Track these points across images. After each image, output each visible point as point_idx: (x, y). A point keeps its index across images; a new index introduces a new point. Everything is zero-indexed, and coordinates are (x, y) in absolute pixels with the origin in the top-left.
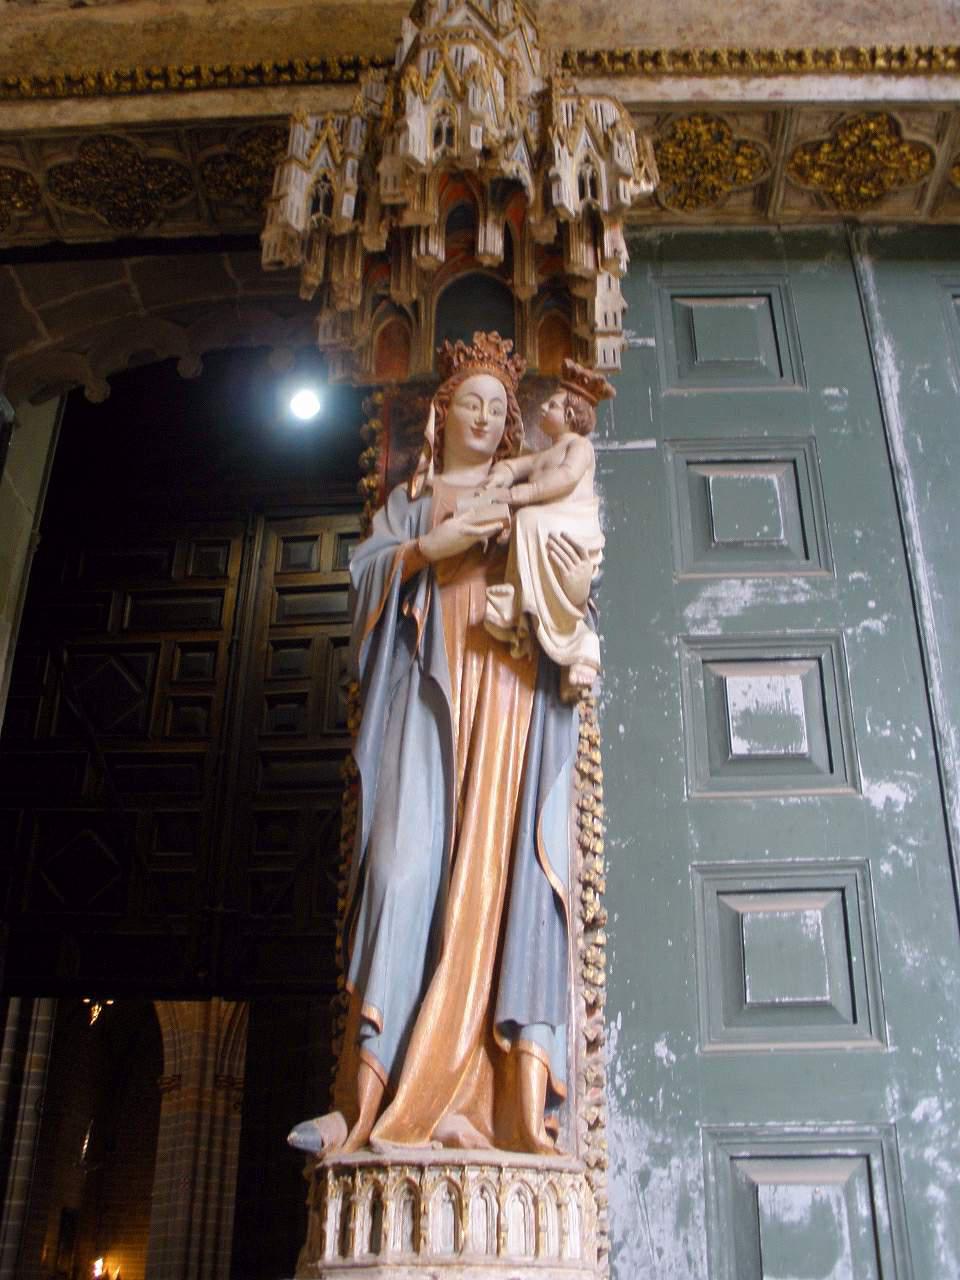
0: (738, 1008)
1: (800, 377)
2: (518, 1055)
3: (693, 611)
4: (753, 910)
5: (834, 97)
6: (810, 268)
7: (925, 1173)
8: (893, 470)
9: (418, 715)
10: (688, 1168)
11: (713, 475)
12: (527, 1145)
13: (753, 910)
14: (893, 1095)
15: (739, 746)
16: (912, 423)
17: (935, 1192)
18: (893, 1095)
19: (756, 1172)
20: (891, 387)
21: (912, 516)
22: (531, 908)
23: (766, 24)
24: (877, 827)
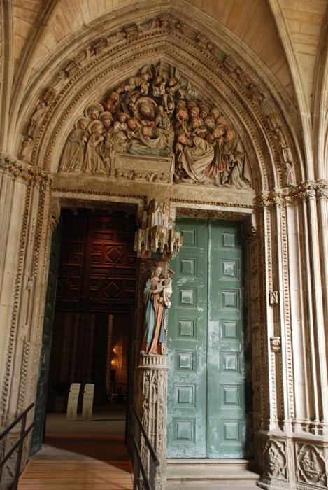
0: (179, 335)
1: (197, 246)
2: (161, 346)
3: (178, 282)
4: (182, 323)
5: (208, 209)
6: (202, 226)
7: (200, 355)
8: (208, 263)
9: (152, 310)
10: (172, 354)
11: (183, 261)
12: (161, 354)
13: (182, 323)
14: (197, 347)
15: (183, 302)
16: (212, 255)
17: (200, 358)
18: (197, 347)
19: (180, 354)
20: (210, 249)
21: (209, 271)
22: (162, 331)
24: (198, 314)
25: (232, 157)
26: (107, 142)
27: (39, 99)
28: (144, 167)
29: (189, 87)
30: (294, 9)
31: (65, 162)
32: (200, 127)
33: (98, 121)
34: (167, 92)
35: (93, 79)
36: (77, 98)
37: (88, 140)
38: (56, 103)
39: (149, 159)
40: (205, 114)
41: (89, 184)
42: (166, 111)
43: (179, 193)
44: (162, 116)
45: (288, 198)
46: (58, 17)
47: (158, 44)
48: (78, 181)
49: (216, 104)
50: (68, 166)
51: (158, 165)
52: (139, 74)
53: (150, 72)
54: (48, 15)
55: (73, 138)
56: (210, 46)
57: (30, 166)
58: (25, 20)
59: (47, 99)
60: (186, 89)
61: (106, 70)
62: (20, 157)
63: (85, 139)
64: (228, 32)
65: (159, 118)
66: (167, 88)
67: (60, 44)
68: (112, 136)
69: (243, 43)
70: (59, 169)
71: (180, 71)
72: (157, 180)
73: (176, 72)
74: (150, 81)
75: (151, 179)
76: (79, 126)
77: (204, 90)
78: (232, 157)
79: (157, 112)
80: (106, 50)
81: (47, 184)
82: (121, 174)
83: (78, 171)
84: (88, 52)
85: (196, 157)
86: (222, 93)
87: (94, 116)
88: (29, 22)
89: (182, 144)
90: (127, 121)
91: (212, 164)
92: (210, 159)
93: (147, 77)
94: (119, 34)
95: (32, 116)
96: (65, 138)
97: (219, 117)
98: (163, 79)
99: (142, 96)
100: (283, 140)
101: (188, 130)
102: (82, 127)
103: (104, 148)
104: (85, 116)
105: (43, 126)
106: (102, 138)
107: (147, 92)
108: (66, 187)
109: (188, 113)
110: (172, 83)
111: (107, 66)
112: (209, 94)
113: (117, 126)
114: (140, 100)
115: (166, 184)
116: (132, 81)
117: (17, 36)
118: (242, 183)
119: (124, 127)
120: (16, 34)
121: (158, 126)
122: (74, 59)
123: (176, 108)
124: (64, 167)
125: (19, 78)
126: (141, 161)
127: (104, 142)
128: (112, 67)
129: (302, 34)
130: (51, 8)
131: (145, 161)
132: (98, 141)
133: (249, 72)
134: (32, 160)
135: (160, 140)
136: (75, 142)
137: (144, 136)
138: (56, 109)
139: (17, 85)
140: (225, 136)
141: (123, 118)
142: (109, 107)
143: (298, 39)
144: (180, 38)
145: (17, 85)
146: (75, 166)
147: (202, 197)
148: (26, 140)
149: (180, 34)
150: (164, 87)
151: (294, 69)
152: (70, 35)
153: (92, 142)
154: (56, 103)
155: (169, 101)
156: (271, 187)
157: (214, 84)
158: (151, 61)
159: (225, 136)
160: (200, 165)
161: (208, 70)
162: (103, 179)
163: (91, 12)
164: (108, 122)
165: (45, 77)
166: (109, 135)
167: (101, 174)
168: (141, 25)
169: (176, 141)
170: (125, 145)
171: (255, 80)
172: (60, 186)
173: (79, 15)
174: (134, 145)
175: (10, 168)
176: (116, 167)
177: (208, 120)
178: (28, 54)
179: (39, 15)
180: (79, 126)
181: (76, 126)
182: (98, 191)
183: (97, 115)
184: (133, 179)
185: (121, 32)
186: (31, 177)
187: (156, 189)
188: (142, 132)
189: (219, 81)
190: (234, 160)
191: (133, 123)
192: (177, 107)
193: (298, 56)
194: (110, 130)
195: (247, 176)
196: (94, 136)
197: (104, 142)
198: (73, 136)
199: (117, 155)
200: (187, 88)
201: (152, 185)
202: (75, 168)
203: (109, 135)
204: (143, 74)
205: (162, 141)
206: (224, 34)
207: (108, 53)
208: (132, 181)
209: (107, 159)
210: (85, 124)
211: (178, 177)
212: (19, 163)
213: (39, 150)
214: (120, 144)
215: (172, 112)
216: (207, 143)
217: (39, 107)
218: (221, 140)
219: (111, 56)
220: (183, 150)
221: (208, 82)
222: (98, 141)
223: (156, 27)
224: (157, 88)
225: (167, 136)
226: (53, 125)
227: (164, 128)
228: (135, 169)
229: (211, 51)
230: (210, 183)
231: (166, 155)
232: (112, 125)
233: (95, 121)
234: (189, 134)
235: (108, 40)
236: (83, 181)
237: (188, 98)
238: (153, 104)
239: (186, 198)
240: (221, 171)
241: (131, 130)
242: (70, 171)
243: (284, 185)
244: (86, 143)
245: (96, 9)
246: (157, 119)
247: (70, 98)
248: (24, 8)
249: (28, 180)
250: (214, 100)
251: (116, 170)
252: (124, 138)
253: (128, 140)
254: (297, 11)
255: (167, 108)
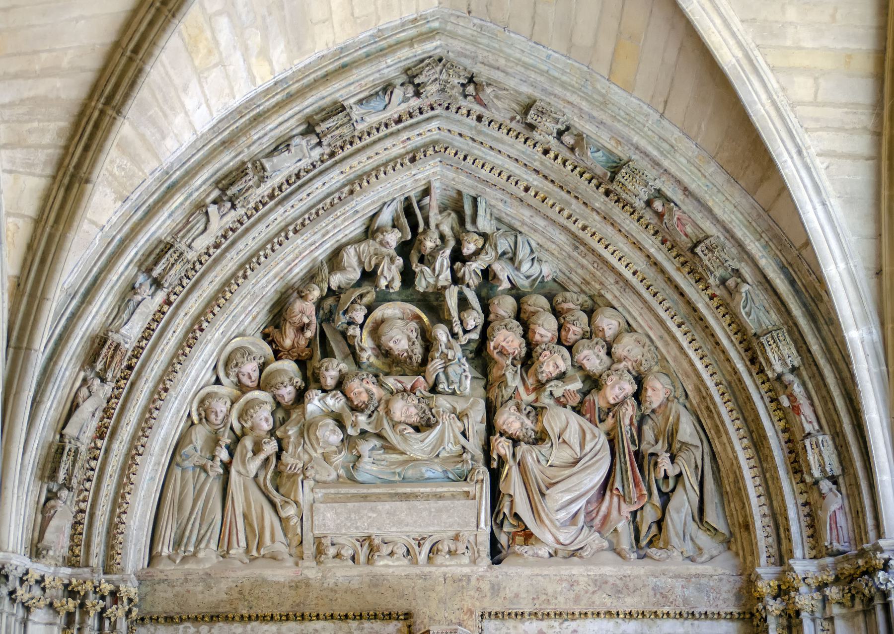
23: (571, 595)
25: (664, 462)
26: (287, 458)
27: (82, 368)
28: (400, 522)
29: (523, 252)
30: (789, 43)
31: (168, 533)
32: (562, 376)
33: (257, 394)
34: (456, 280)
35: (234, 275)
36: (189, 340)
37: (231, 455)
38: (130, 368)
39: (416, 496)
40: (574, 331)
41: (240, 592)
42: (454, 335)
43: (509, 593)
44: (444, 356)
45: (833, 592)
46: (124, 148)
47: (417, 141)
48: (210, 588)
49: (609, 296)
50: (177, 544)
51: (439, 511)
52: (370, 232)
53: (404, 221)
54: (90, 154)
55: (188, 457)
56: (568, 139)
57: (69, 571)
58: (34, 175)
59: (105, 370)
60: (512, 258)
61: (270, 241)
62: (36, 551)
63: (224, 455)
64: (617, 94)
65: (435, 365)
66: (458, 264)
67: (129, 203)
68: (301, 434)
69: (665, 123)
70: (153, 558)
71: (491, 206)
72: (439, 559)
73: (481, 211)
74: (404, 249)
75: (423, 557)
76: (205, 418)
77: (570, 257)
78: (664, 462)
79: (428, 343)
80: (264, 189)
81: (121, 613)
82: (332, 551)
83: (209, 554)
84: (213, 209)
85: (551, 472)
86: (620, 267)
87: (245, 380)
88: (40, 176)
89: (510, 437)
90: (340, 385)
91: (606, 485)
92: (598, 476)
93: (393, 238)
94: (297, 140)
95: (63, 428)
96: (165, 459)
97: (617, 337)
98: (442, 237)
99: (383, 298)
100: (806, 409)
101: (527, 389)
102: (212, 417)
103: (278, 473)
104: (218, 382)
105: (99, 443)
106: (271, 447)
107: (397, 284)
108: (173, 609)
109: (525, 336)
110: (469, 249)
111: (274, 229)
112: (583, 267)
113: (315, 403)
114: (377, 314)
115: (466, 570)
116: (350, 257)
117: (10, 220)
118: (703, 539)
119: (335, 402)
120: (8, 214)
121: (434, 389)
122: (175, 234)
123: (487, 324)
124: (165, 550)
125: (23, 328)
126: (388, 506)
127: (278, 456)
128: (285, 229)
129: (825, 104)
130: (99, 134)
131: (403, 505)
132: (262, 456)
133: (688, 206)
134: (71, 549)
135: (442, 433)
136: (195, 466)
137: (394, 425)
138: (133, 385)
139: (17, 349)
140: (638, 396)
141: (330, 377)
142: (288, 343)
143: (817, 120)
144: (479, 119)
145: (17, 349)
146: (199, 541)
147: (577, 599)
148: (52, 496)
149: (477, 109)
150: (447, 262)
151: (809, 207)
152: (157, 174)
153: (243, 463)
154: (130, 368)
155: (463, 303)
156: (782, 558)
157: (593, 243)
158: (402, 188)
159: (638, 396)
160: (568, 497)
161: (574, 201)
162: (282, 574)
163: (213, 102)
164: (287, 393)
165: (94, 309)
166: (292, 431)
167: (274, 558)
168: (360, 102)
169: (491, 428)
170: (340, 459)
171: (708, 227)
172: (159, 609)
173: (179, 120)
174: (366, 459)
175: (11, 593)
176: (317, 532)
177: (586, 352)
178: (43, 261)
179: (66, 148)
180: (205, 418)
181: (195, 418)
182: (268, 612)
183: (255, 376)
184: (369, 561)
185: (303, 134)
186: (71, 605)
187: (438, 588)
188: (388, 412)
189: (609, 231)
190: (672, 472)
191: (362, 388)
192: (492, 317)
193: (820, 164)
194: (294, 416)
195: (713, 516)
196: (248, 443)
197: (278, 456)
198: (188, 449)
199: (320, 493)
200: (515, 254)
201: (424, 577)
202: (197, 546)
203: (292, 431)
204: (380, 230)
205: (449, 436)
206: (604, 103)
207: (272, 196)
208: (366, 569)
209: (290, 511)
210: (221, 407)
211: (503, 539)
212: (37, 569)
213: (92, 516)
214: (326, 457)
215: (475, 336)
216: (587, 425)
217: (84, 391)
218: (629, 412)
219: (280, 203)
220: (514, 455)
221: (575, 237)
222: (262, 456)
223: (405, 100)
224: (427, 270)
225: (461, 416)
226: (126, 433)
227: (454, 393)
228: (373, 531)
229: (572, 149)
230: (602, 550)
231: (464, 478)
232: (300, 397)
233: (250, 395)
234: (527, 397)
235: (267, 165)
236: (224, 586)
237: (523, 283)
238: (417, 318)
239: (527, 610)
240: (633, 509)
241: (355, 409)
242: (184, 559)
243: (818, 550)
244: (226, 467)
245: (227, 91)
246: (430, 367)
247: (171, 340)
248: (29, 147)
249: (63, 614)
250: (601, 283)
251: (319, 542)
252: (336, 437)
253: (348, 441)
254: (800, 48)
255: (457, 329)
